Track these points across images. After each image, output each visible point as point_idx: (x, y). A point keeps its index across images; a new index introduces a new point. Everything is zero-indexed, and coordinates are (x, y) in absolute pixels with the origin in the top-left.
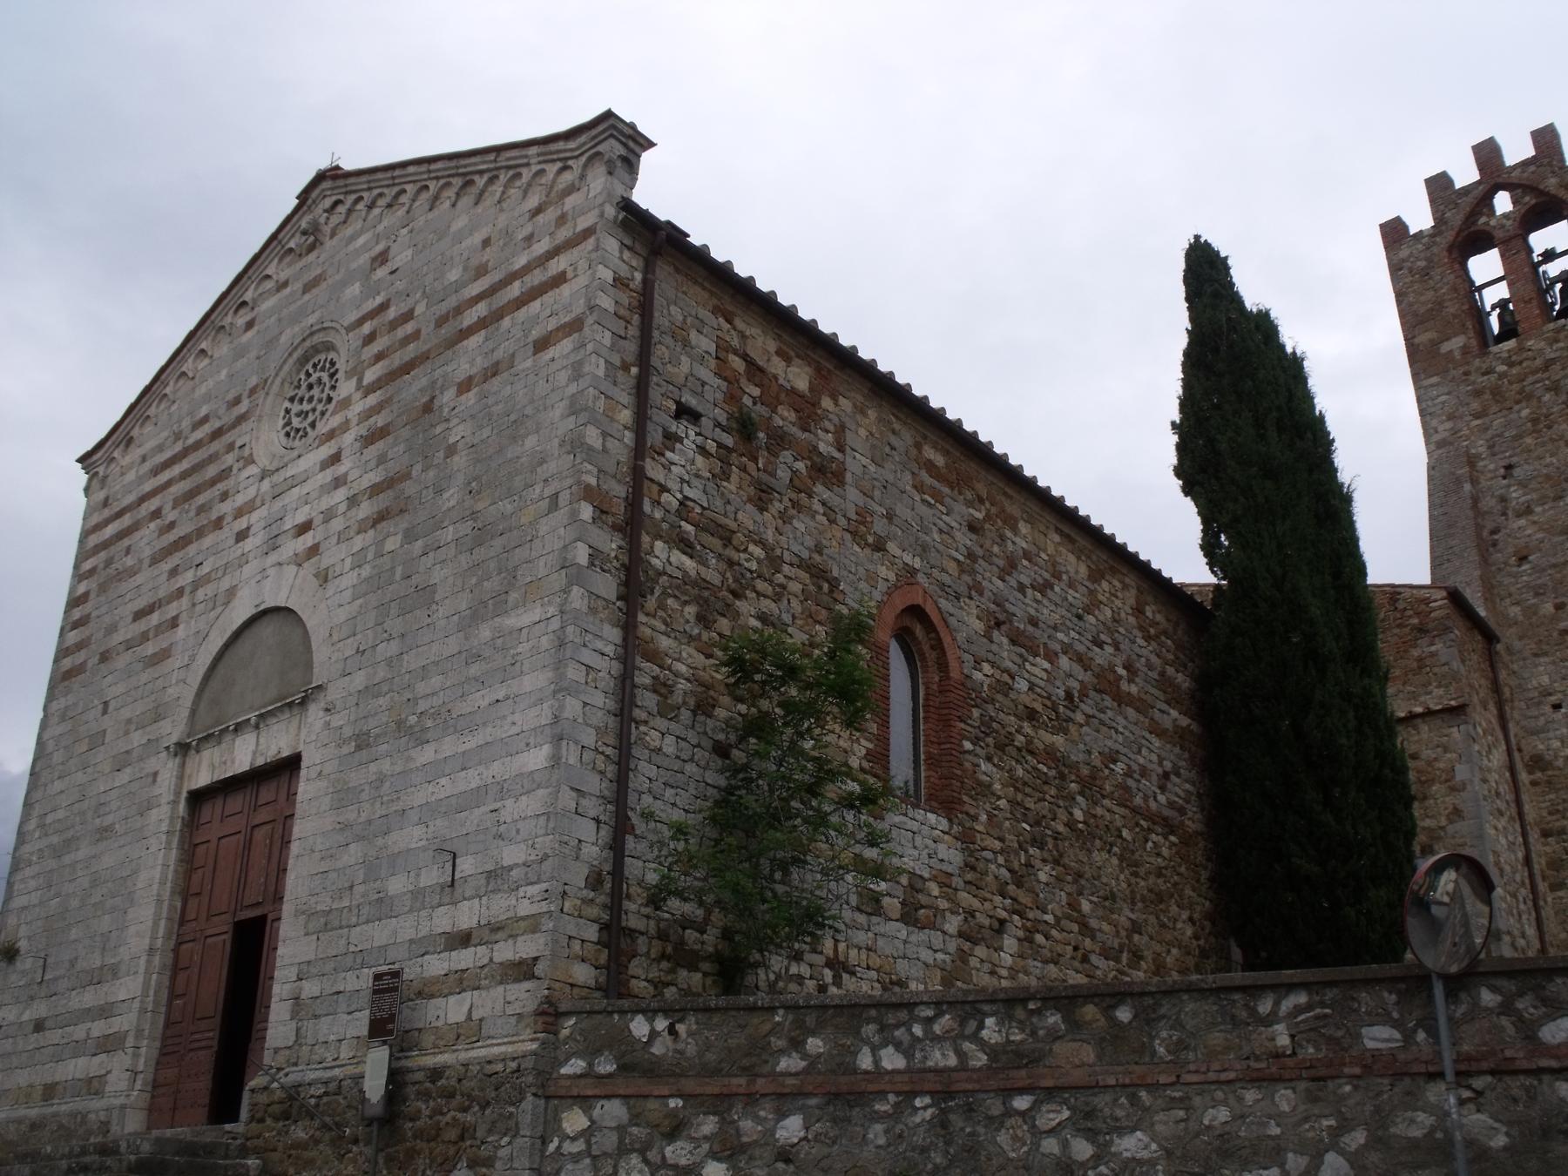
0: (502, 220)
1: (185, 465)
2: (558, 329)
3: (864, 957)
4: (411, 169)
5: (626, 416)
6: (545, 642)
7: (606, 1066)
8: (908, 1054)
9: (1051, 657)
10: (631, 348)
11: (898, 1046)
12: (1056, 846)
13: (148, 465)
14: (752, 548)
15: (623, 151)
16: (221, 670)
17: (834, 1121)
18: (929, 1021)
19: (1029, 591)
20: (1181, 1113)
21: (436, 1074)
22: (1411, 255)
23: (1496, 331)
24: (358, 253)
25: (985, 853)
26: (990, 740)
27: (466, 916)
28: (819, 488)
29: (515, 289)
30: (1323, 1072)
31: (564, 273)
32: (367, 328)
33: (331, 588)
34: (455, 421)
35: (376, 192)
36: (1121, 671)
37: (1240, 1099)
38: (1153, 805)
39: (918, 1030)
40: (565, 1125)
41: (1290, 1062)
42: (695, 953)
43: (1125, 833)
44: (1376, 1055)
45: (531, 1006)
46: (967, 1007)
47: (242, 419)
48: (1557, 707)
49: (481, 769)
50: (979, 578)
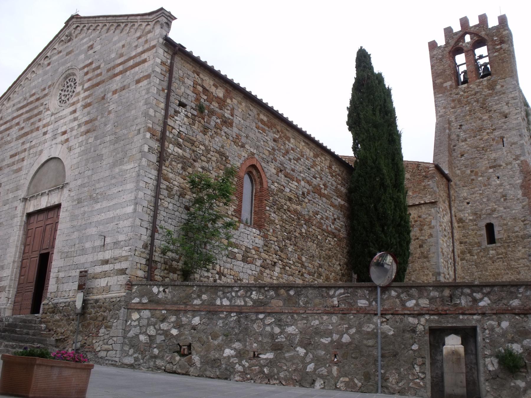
0: (129, 39)
1: (27, 109)
2: (143, 77)
3: (229, 271)
4: (101, 19)
5: (162, 105)
6: (134, 174)
7: (145, 300)
8: (230, 301)
9: (298, 181)
10: (165, 84)
11: (228, 298)
12: (295, 240)
13: (15, 108)
14: (201, 146)
15: (166, 21)
16: (37, 176)
17: (209, 319)
18: (237, 291)
19: (292, 161)
20: (305, 321)
21: (97, 301)
22: (437, 53)
23: (462, 80)
24: (84, 44)
25: (271, 242)
26: (275, 207)
27: (107, 255)
28: (224, 128)
29: (131, 63)
30: (345, 312)
31: (146, 59)
32: (86, 70)
33: (72, 152)
34: (111, 103)
35: (90, 24)
36: (322, 186)
37: (322, 318)
38: (329, 229)
39: (233, 294)
40: (132, 317)
41: (336, 309)
42: (176, 269)
43: (319, 237)
44: (361, 308)
45: (125, 282)
46: (248, 288)
47: (46, 95)
48: (468, 203)
49: (114, 211)
50: (276, 156)
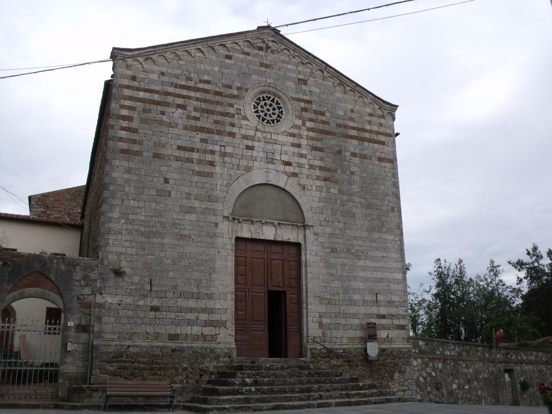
27: (383, 311)
49: (381, 273)
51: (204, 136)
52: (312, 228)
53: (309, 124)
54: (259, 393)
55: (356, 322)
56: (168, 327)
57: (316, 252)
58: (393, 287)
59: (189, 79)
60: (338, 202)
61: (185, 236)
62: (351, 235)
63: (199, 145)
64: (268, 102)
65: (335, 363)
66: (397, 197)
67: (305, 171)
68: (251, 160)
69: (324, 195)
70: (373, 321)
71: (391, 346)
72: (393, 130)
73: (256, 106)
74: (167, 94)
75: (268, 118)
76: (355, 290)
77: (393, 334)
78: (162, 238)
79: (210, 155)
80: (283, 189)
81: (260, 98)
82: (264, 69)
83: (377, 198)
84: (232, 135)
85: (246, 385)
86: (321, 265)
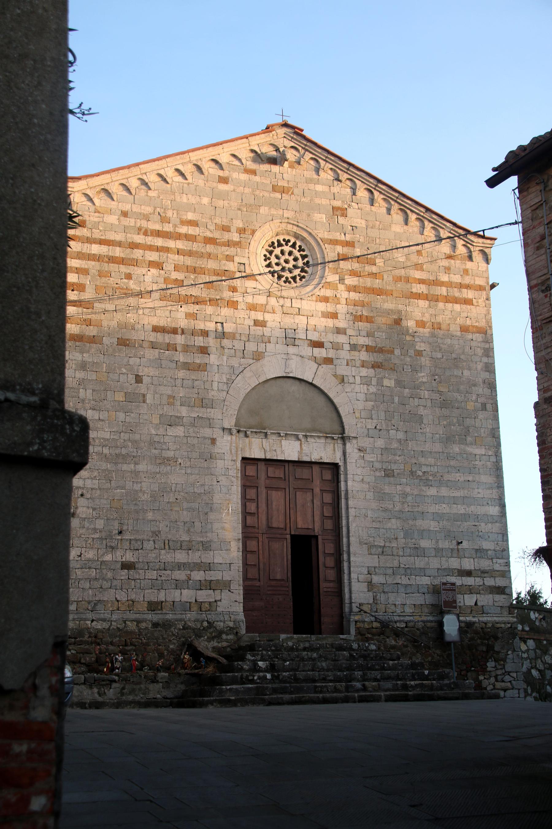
27: (468, 564)
49: (465, 506)
51: (193, 308)
52: (354, 441)
53: (350, 281)
54: (277, 681)
55: (425, 581)
56: (147, 591)
57: (361, 477)
58: (483, 527)
59: (164, 220)
60: (396, 399)
61: (168, 459)
62: (416, 449)
63: (183, 323)
64: (287, 249)
65: (393, 642)
66: (492, 386)
67: (345, 354)
68: (263, 342)
69: (373, 389)
70: (452, 579)
71: (481, 619)
72: (488, 278)
73: (268, 256)
74: (134, 246)
75: (287, 274)
76: (422, 533)
77: (485, 600)
78: (136, 464)
79: (201, 338)
80: (311, 384)
81: (273, 243)
82: (278, 195)
83: (458, 391)
84: (233, 304)
85: (260, 670)
86: (370, 495)
